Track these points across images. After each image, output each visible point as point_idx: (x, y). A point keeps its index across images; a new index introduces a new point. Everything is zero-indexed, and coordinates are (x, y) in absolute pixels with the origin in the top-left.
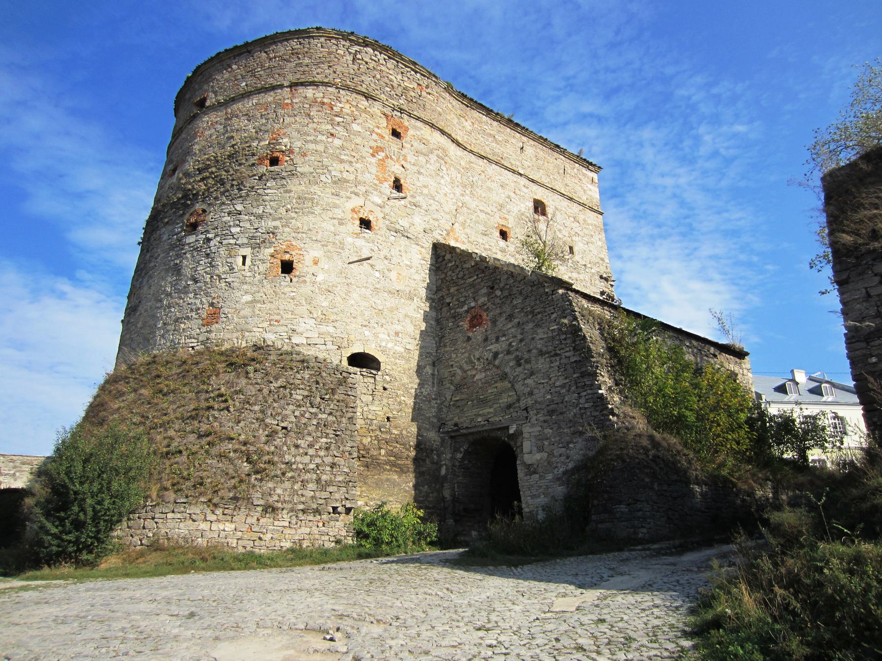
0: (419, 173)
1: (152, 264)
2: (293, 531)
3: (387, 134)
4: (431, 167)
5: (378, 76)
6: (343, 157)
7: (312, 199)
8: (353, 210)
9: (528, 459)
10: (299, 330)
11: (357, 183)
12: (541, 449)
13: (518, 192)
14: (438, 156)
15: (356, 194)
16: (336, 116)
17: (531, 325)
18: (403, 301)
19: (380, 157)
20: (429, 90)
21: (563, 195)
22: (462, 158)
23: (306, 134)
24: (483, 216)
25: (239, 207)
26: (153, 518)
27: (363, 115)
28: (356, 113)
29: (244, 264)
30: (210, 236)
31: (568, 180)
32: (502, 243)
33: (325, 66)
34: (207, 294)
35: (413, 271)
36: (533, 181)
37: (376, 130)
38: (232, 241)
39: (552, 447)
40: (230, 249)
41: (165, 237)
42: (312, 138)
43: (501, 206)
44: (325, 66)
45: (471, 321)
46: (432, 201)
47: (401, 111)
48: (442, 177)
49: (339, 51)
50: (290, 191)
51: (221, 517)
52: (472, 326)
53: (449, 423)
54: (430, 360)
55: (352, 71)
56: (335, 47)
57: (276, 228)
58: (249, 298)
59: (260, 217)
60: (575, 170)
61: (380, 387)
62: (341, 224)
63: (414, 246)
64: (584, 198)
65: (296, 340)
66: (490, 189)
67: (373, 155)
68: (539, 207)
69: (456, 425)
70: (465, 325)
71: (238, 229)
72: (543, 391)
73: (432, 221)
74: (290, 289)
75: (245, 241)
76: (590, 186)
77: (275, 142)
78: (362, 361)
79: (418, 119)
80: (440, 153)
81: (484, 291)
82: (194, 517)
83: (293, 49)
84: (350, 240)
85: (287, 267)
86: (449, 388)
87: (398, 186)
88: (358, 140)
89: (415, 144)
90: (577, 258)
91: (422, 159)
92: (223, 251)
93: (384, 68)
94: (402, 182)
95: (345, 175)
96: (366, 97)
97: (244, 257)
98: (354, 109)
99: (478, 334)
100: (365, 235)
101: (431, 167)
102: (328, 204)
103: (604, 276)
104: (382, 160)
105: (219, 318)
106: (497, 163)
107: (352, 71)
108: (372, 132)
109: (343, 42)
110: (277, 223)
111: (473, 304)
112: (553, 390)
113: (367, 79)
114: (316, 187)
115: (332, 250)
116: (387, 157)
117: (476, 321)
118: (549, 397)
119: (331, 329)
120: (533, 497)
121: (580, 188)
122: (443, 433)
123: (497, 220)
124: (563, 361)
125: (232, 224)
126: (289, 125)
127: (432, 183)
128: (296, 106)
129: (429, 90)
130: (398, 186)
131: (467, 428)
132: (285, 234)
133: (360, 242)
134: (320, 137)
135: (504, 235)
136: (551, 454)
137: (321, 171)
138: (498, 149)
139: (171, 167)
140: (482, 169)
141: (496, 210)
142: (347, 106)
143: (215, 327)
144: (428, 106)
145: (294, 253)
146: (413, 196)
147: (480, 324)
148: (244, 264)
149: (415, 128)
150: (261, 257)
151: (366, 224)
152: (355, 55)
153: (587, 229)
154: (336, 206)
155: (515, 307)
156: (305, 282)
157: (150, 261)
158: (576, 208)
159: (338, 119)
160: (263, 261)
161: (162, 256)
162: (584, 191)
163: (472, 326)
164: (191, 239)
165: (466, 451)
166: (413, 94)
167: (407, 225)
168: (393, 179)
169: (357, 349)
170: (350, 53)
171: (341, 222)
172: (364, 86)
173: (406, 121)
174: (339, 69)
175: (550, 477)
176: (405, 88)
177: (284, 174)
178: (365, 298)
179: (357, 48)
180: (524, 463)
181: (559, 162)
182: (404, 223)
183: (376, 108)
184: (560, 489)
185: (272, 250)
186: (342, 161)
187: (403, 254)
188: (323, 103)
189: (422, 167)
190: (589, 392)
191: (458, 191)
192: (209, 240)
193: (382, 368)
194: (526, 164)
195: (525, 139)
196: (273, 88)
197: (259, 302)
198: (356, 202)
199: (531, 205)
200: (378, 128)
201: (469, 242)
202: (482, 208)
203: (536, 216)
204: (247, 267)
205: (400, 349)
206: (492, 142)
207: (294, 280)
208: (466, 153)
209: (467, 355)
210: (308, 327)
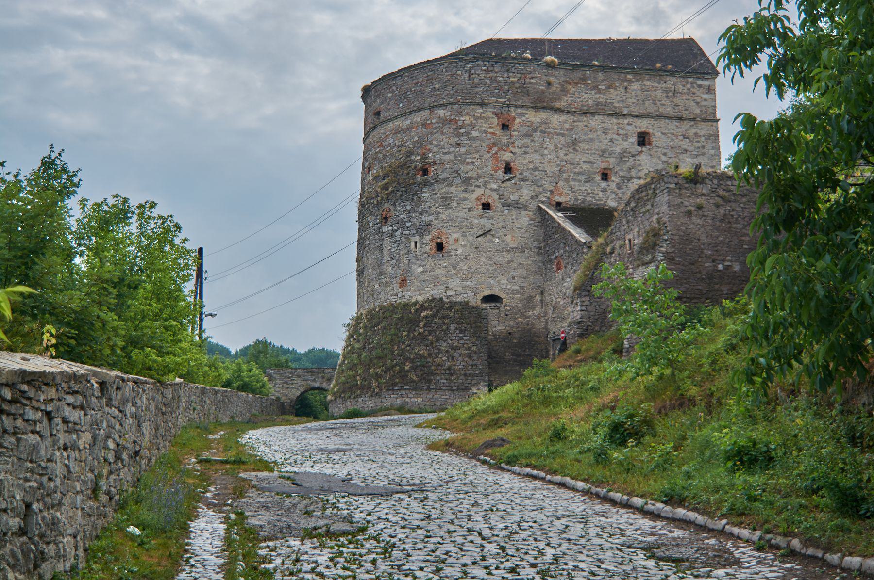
0: (526, 153)
3: (498, 131)
6: (467, 160)
8: (477, 199)
11: (479, 177)
13: (621, 132)
14: (541, 132)
15: (479, 186)
20: (532, 75)
21: (670, 118)
22: (565, 122)
23: (442, 148)
24: (586, 167)
25: (409, 208)
27: (479, 121)
30: (395, 228)
31: (677, 100)
32: (604, 184)
33: (449, 88)
35: (522, 231)
37: (490, 130)
38: (408, 232)
41: (371, 225)
42: (446, 150)
43: (604, 152)
44: (449, 88)
46: (537, 173)
47: (508, 106)
48: (546, 148)
49: (459, 72)
50: (436, 194)
52: (558, 269)
55: (469, 87)
56: (455, 69)
57: (431, 221)
58: (421, 269)
59: (421, 214)
60: (689, 86)
62: (470, 211)
65: (449, 293)
66: (592, 140)
67: (488, 152)
68: (643, 139)
73: (537, 189)
75: (415, 232)
76: (705, 96)
77: (424, 157)
81: (562, 246)
84: (476, 221)
85: (440, 247)
87: (508, 169)
91: (527, 140)
94: (512, 164)
95: (470, 174)
97: (416, 242)
98: (472, 119)
99: (559, 275)
102: (460, 199)
104: (496, 153)
106: (599, 114)
107: (469, 87)
108: (486, 132)
110: (431, 218)
114: (452, 188)
116: (499, 150)
121: (693, 104)
127: (536, 157)
130: (508, 169)
133: (483, 221)
134: (453, 149)
135: (605, 177)
138: (602, 98)
139: (366, 164)
140: (586, 123)
141: (597, 157)
146: (521, 174)
150: (425, 241)
151: (486, 206)
152: (470, 70)
153: (698, 142)
154: (465, 199)
158: (686, 125)
159: (462, 131)
160: (426, 244)
162: (698, 103)
164: (386, 229)
166: (517, 85)
169: (487, 292)
171: (470, 210)
178: (490, 258)
181: (669, 84)
185: (430, 237)
186: (468, 164)
187: (515, 221)
188: (451, 120)
189: (528, 147)
195: (630, 76)
196: (420, 110)
198: (479, 192)
199: (634, 139)
200: (491, 128)
201: (573, 192)
203: (639, 149)
205: (516, 287)
206: (596, 93)
207: (445, 255)
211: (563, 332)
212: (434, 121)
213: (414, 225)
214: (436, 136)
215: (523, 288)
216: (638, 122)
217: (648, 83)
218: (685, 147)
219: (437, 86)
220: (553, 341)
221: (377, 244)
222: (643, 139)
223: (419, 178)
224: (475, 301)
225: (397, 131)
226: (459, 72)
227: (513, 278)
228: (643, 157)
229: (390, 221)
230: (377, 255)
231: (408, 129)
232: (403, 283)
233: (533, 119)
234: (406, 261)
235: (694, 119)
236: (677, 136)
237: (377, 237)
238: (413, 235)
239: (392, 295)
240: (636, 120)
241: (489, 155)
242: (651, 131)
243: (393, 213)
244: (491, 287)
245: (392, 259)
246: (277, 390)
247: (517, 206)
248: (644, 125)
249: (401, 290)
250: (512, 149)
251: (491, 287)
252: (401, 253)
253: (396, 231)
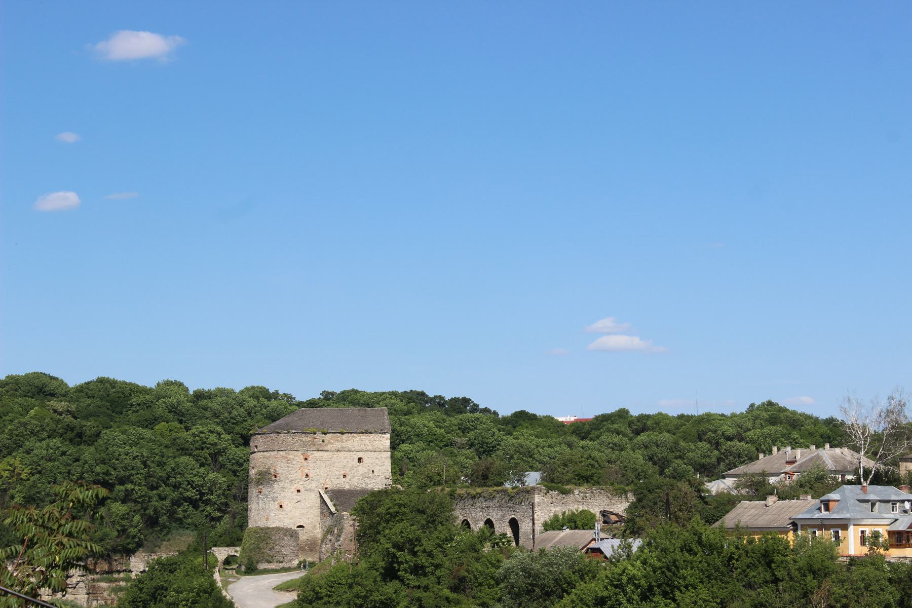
68: (360, 460)
85: (281, 506)
87: (307, 476)
123: (343, 472)
130: (307, 476)
135: (345, 476)
138: (344, 445)
151: (298, 491)
183: (299, 454)
222: (360, 460)
223: (273, 478)
232: (267, 519)
247: (310, 490)
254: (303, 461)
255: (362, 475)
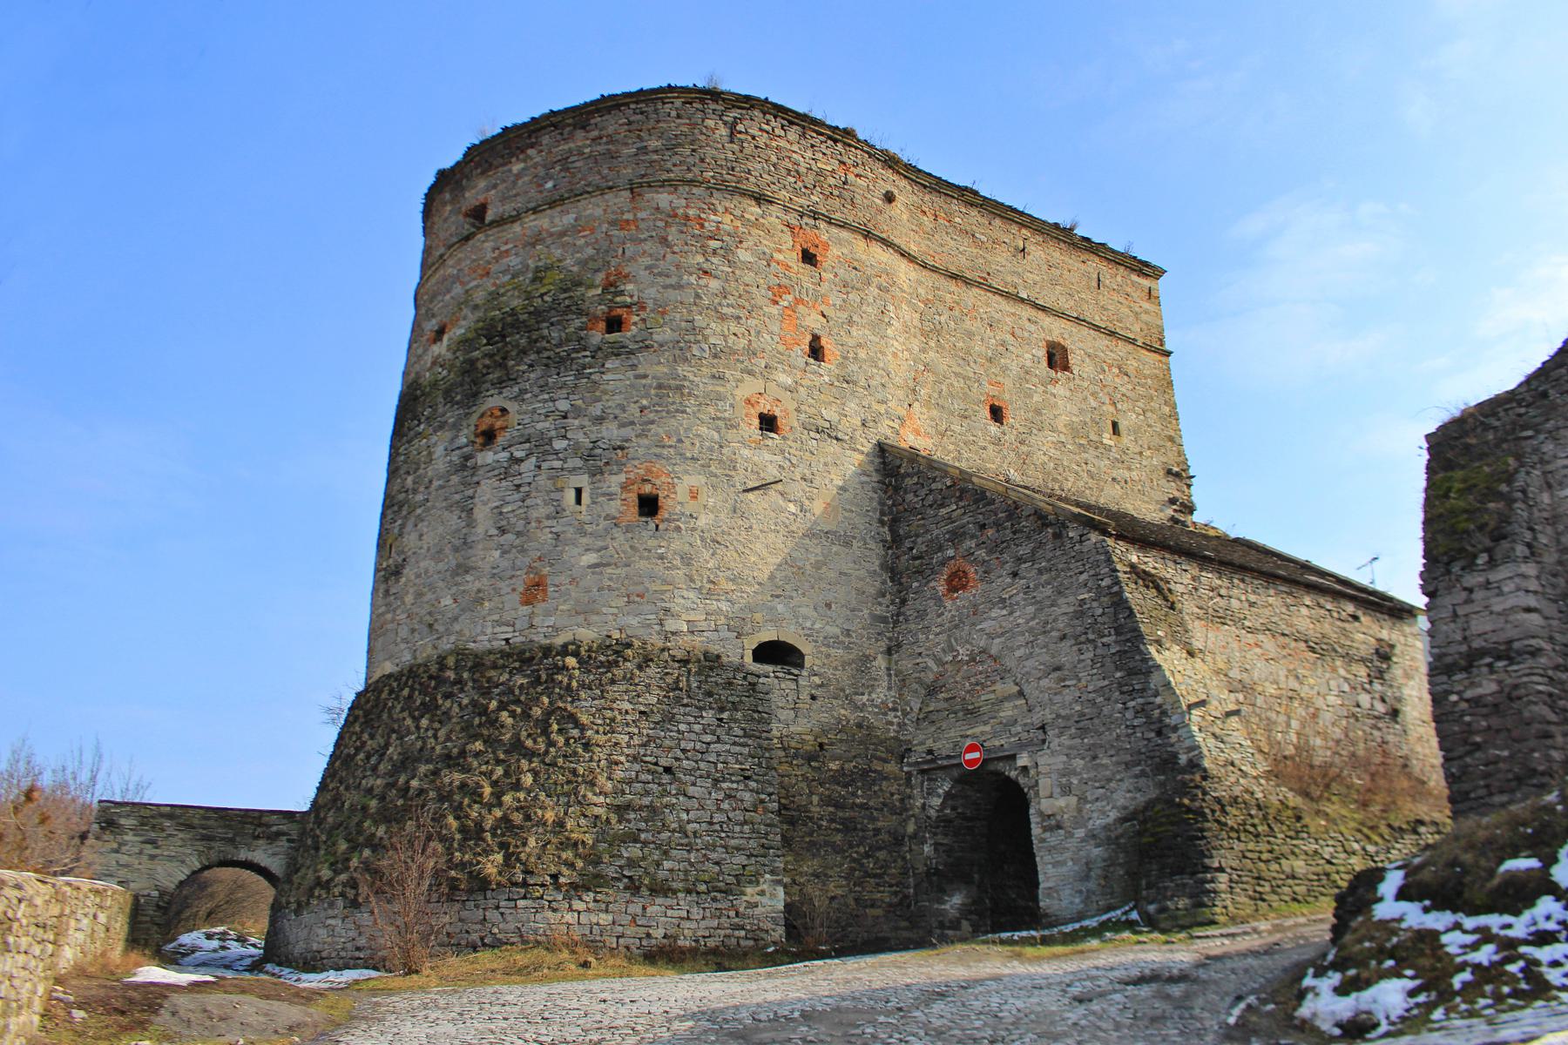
1: (420, 497)
2: (694, 925)
4: (870, 309)
5: (773, 158)
6: (725, 310)
7: (680, 388)
9: (1046, 805)
10: (676, 609)
12: (1066, 790)
15: (751, 373)
16: (711, 238)
17: (1048, 591)
18: (835, 549)
19: (786, 304)
20: (858, 170)
21: (1097, 328)
23: (660, 274)
25: (563, 405)
26: (498, 907)
27: (755, 231)
28: (742, 229)
29: (579, 501)
30: (519, 454)
31: (1105, 298)
32: (994, 428)
34: (523, 551)
36: (1043, 309)
38: (557, 464)
39: (1084, 787)
40: (555, 474)
41: (439, 451)
42: (673, 280)
45: (949, 581)
47: (815, 216)
50: (645, 376)
51: (591, 905)
52: (953, 589)
53: (919, 748)
54: (883, 644)
55: (730, 155)
58: (591, 558)
59: (599, 420)
60: (1119, 279)
61: (805, 696)
63: (848, 453)
64: (1136, 328)
65: (671, 625)
68: (1057, 358)
69: (930, 752)
70: (941, 588)
71: (564, 444)
72: (1068, 698)
73: (875, 406)
74: (652, 543)
76: (1146, 305)
78: (777, 653)
79: (843, 226)
80: (883, 281)
82: (554, 905)
83: (630, 123)
84: (746, 452)
85: (649, 506)
86: (916, 691)
88: (749, 277)
89: (841, 272)
90: (1126, 440)
92: (542, 480)
93: (783, 143)
94: (823, 342)
96: (756, 199)
97: (579, 491)
98: (738, 223)
100: (769, 442)
101: (870, 309)
102: (706, 395)
103: (1176, 469)
105: (545, 591)
106: (979, 285)
109: (713, 106)
110: (627, 432)
111: (950, 553)
112: (1084, 697)
113: (756, 166)
115: (718, 472)
116: (798, 301)
117: (957, 582)
118: (1078, 708)
119: (724, 606)
120: (1056, 864)
122: (909, 765)
124: (1099, 651)
125: (553, 433)
126: (632, 259)
128: (642, 225)
129: (858, 170)
130: (816, 352)
131: (948, 757)
132: (639, 448)
135: (997, 414)
136: (1082, 799)
137: (692, 338)
139: (431, 325)
142: (728, 218)
143: (540, 607)
144: (858, 200)
145: (658, 482)
147: (964, 587)
148: (579, 501)
149: (840, 242)
151: (768, 423)
155: (1020, 560)
156: (678, 529)
157: (415, 491)
158: (1123, 348)
159: (714, 244)
160: (610, 496)
161: (436, 483)
163: (953, 589)
164: (487, 457)
165: (948, 795)
166: (831, 181)
167: (834, 417)
168: (809, 338)
170: (725, 123)
172: (752, 179)
173: (825, 233)
174: (710, 152)
175: (1080, 833)
176: (820, 173)
177: (632, 346)
179: (735, 113)
180: (1040, 813)
182: (830, 414)
183: (774, 217)
184: (1097, 851)
185: (622, 478)
190: (1140, 701)
191: (915, 345)
192: (519, 461)
193: (807, 665)
194: (1030, 277)
197: (608, 565)
198: (751, 387)
199: (1042, 353)
200: (780, 251)
202: (958, 370)
204: (583, 508)
208: (925, 273)
209: (943, 637)
210: (689, 604)
211: (972, 749)
212: (640, 215)
213: (576, 448)
214: (647, 246)
215: (848, 633)
216: (1046, 320)
217: (1057, 254)
218: (1123, 390)
219: (654, 143)
220: (923, 772)
221: (457, 497)
222: (1057, 358)
223: (597, 336)
224: (740, 652)
225: (537, 239)
226: (710, 123)
227: (828, 606)
228: (1059, 390)
229: (501, 440)
230: (454, 520)
231: (563, 234)
232: (534, 591)
233: (864, 257)
234: (546, 537)
235: (1132, 342)
236: (1110, 366)
237: (455, 479)
238: (573, 470)
239: (499, 623)
240: (1041, 315)
241: (774, 310)
242: (1067, 344)
243: (514, 417)
244: (776, 621)
245: (503, 531)
246: (124, 859)
248: (1057, 330)
249: (526, 610)
250: (823, 308)
251: (776, 621)
252: (534, 514)
253: (519, 461)
254: (793, 258)
255: (1075, 431)
